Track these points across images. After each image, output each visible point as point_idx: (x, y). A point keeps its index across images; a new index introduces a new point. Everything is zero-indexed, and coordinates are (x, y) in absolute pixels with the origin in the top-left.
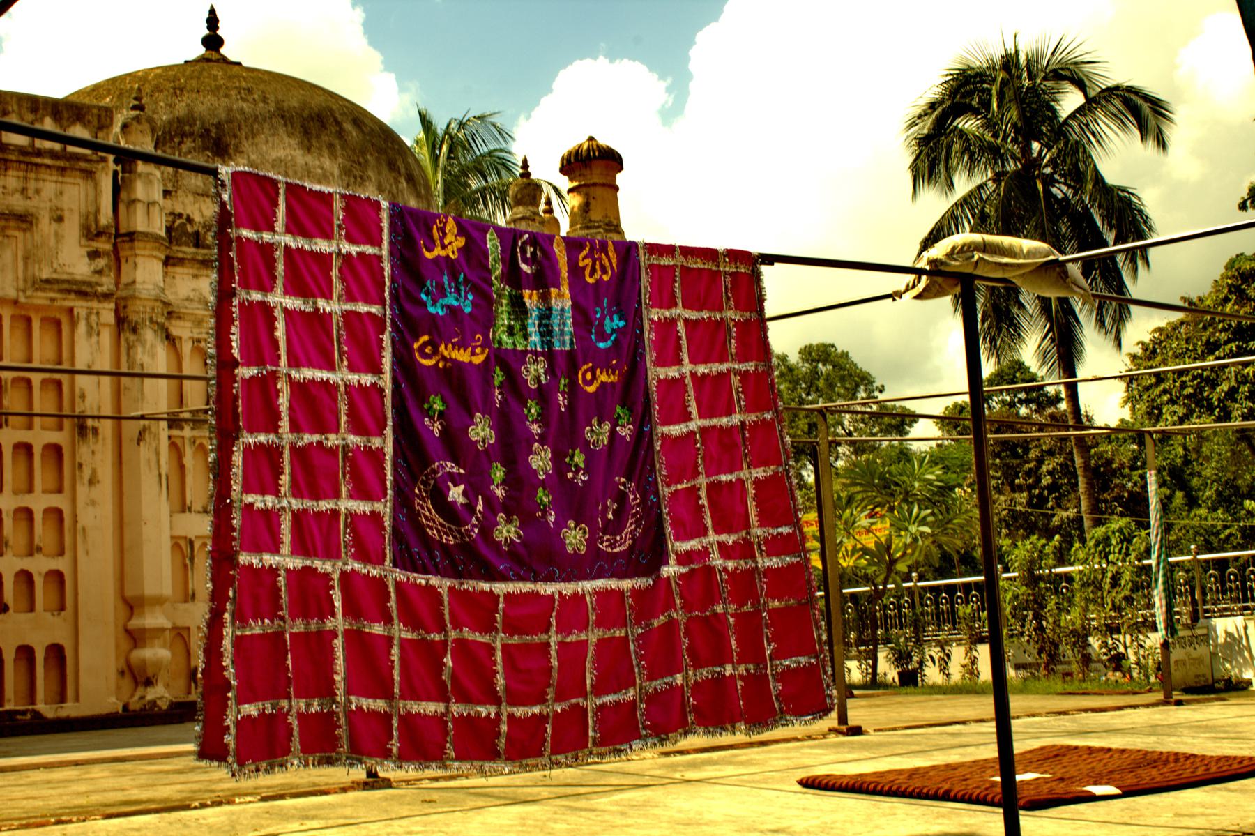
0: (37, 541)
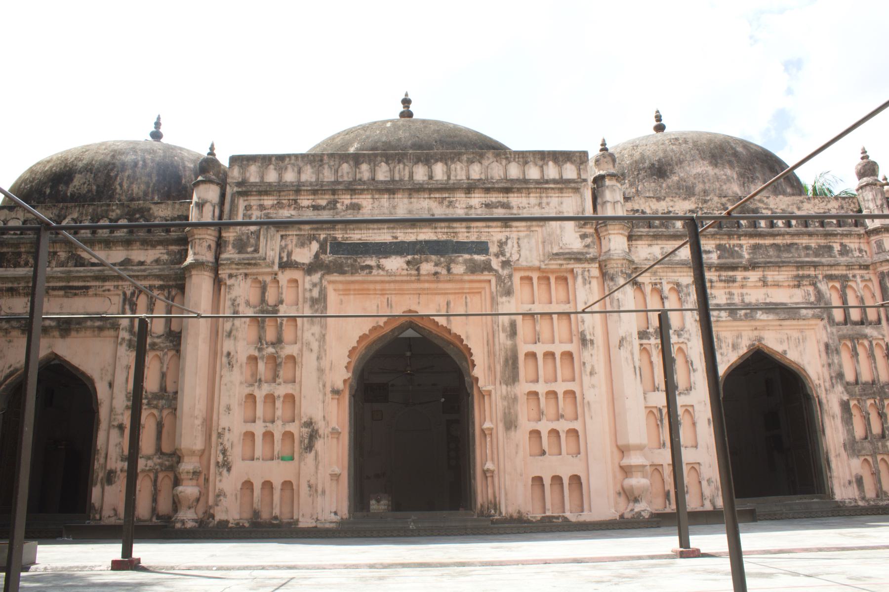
0: (560, 411)
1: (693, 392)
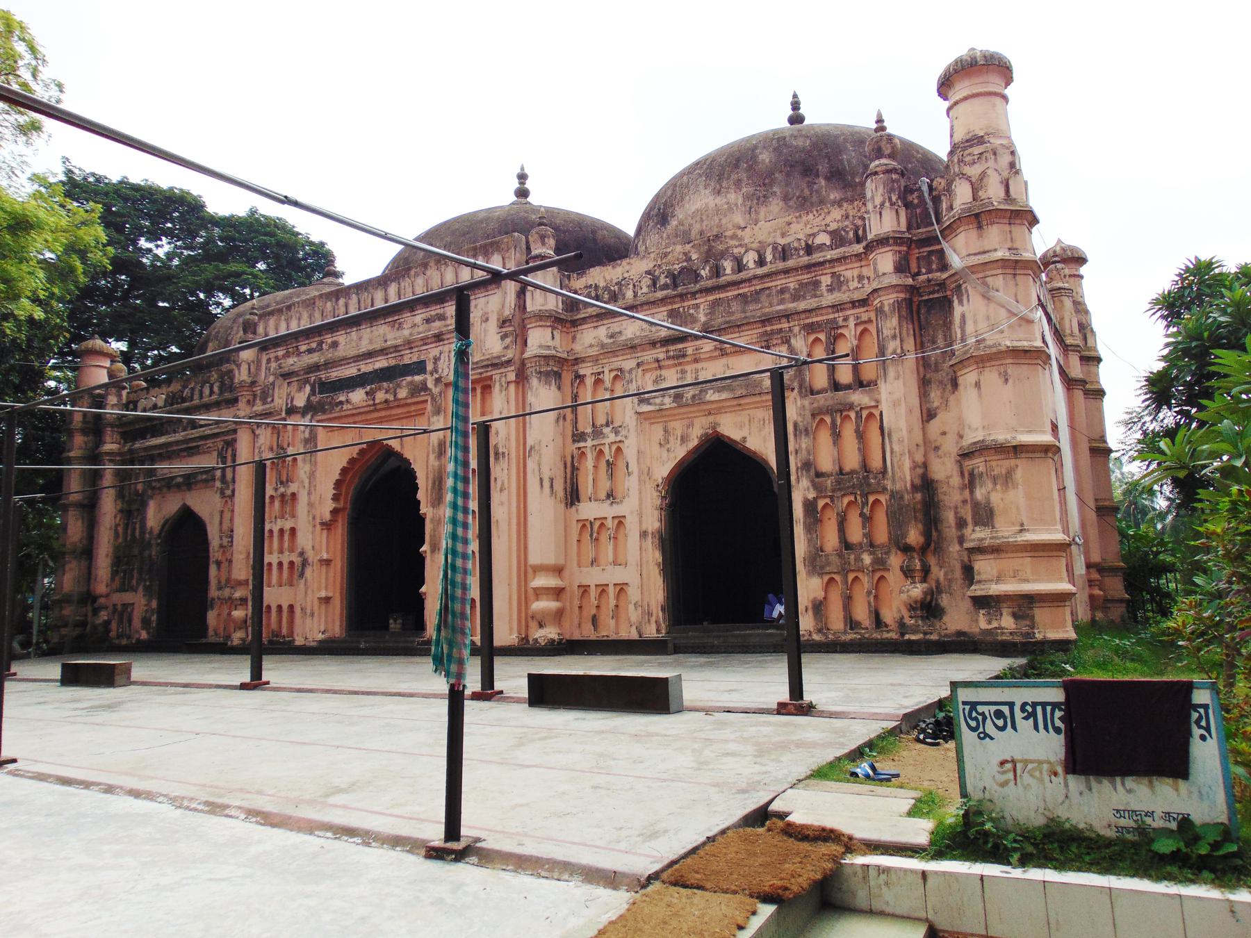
1: (626, 501)
